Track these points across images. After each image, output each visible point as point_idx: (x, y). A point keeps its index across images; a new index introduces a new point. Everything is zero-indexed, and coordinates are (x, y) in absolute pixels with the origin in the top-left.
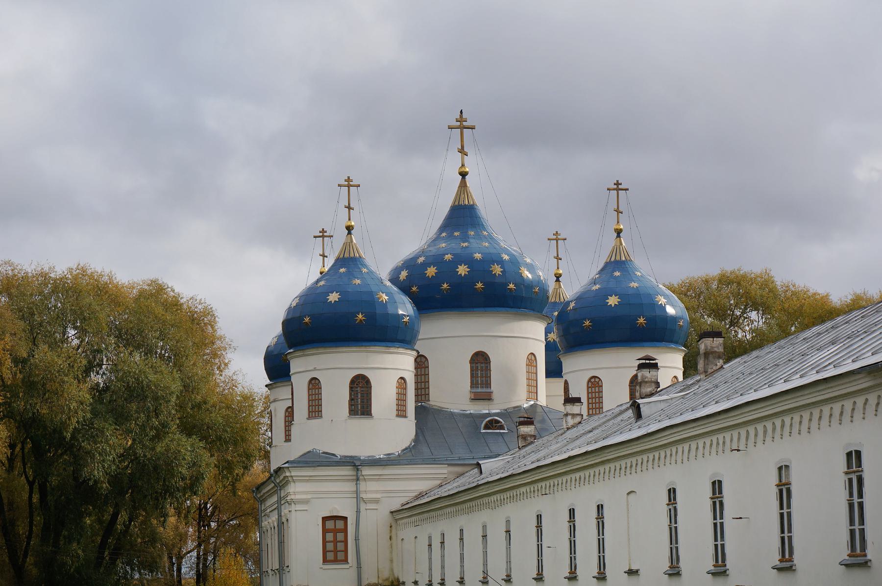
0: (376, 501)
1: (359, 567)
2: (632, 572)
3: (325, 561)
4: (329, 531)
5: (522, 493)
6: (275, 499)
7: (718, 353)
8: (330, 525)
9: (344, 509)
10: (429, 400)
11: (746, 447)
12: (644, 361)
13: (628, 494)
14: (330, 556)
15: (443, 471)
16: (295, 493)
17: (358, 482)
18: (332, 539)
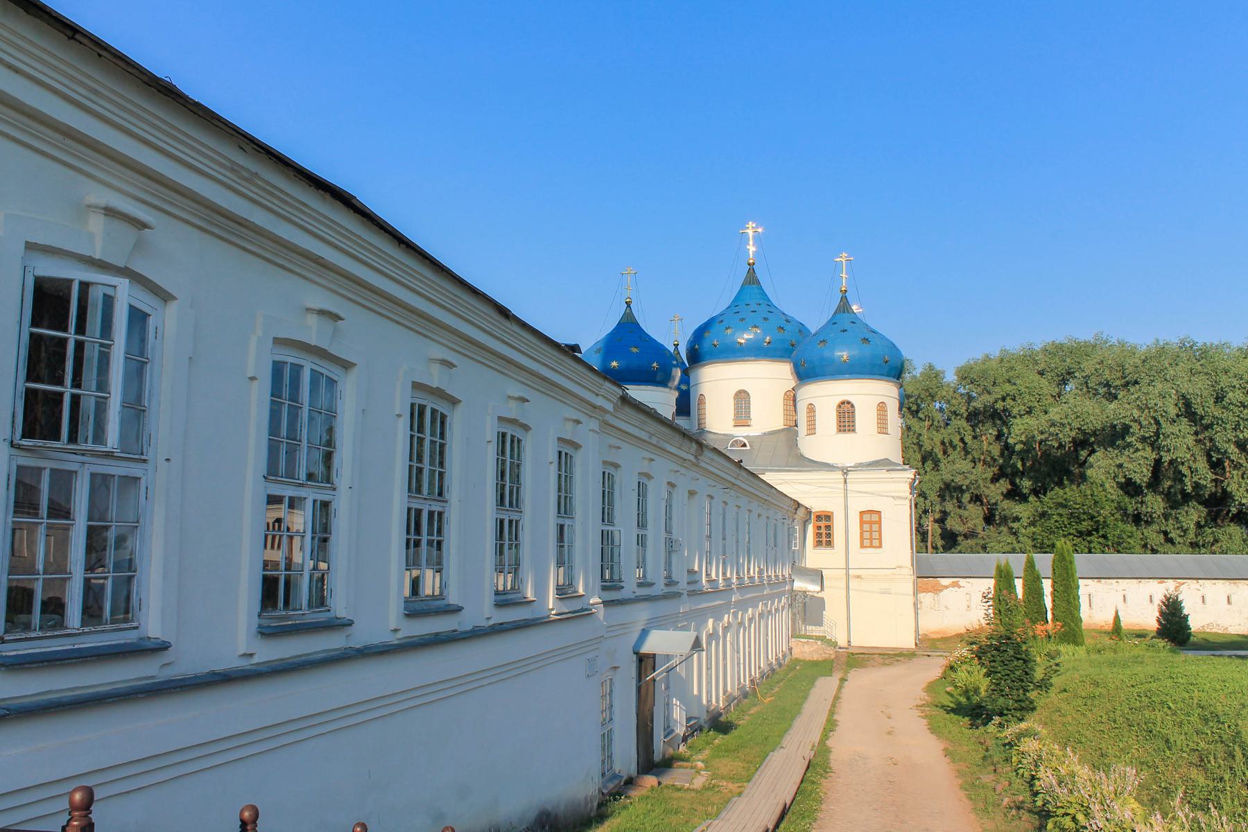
3: (862, 546)
4: (866, 522)
8: (866, 517)
14: (867, 543)
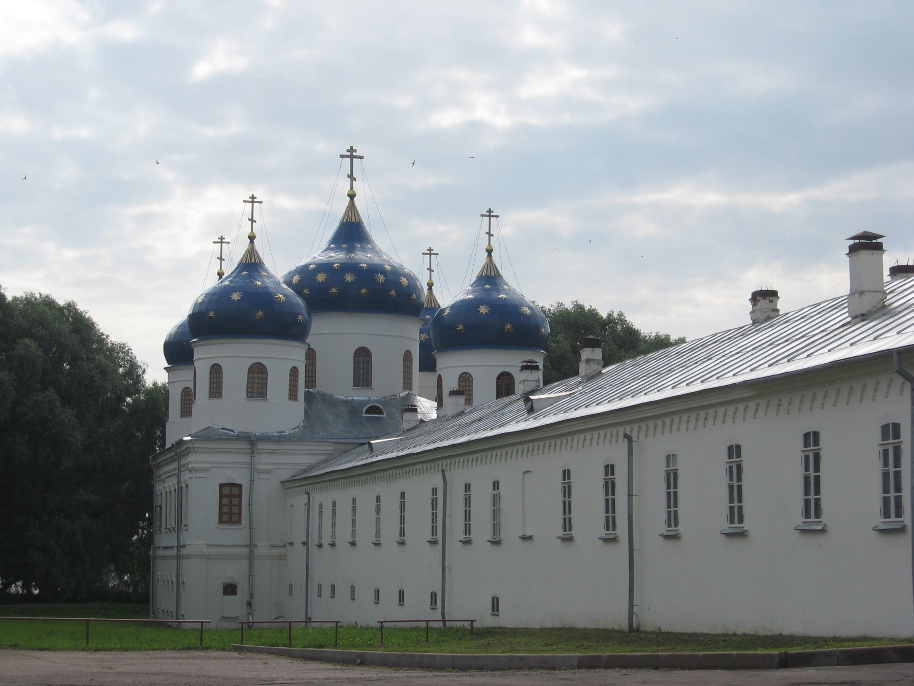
0: (269, 472)
1: (251, 528)
2: (526, 538)
3: (221, 521)
5: (418, 469)
6: (174, 465)
7: (598, 360)
8: (226, 491)
9: (239, 476)
10: (315, 386)
11: (638, 439)
12: (526, 364)
13: (524, 473)
14: (226, 518)
15: (329, 448)
16: (196, 462)
17: (253, 455)
18: (227, 503)
